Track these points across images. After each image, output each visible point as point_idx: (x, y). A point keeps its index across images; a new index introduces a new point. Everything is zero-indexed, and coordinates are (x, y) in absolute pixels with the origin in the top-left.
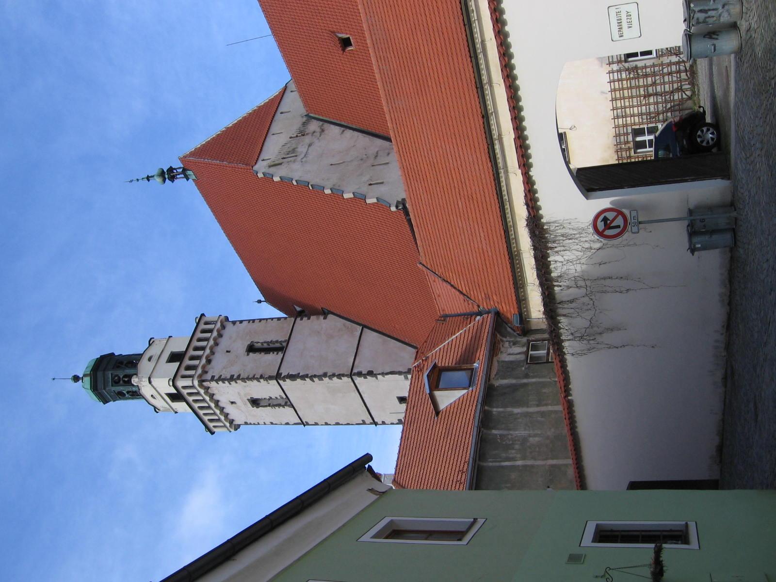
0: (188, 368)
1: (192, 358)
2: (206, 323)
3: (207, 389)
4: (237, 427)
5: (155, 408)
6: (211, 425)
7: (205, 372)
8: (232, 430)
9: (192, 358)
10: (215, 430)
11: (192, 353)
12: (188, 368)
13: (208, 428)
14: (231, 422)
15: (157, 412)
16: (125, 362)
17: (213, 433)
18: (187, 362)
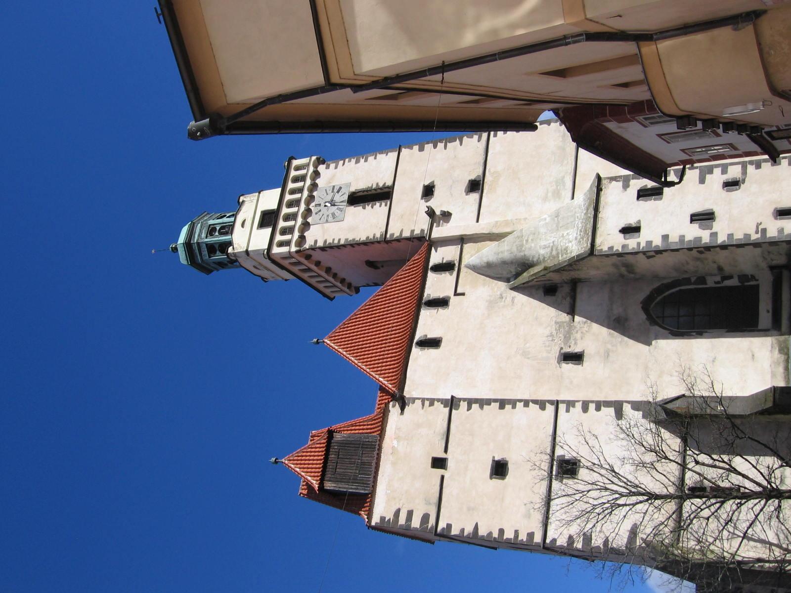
0: (284, 232)
1: (287, 218)
2: (298, 168)
3: (308, 257)
4: (357, 290)
5: (263, 278)
6: (328, 291)
7: (302, 238)
8: (355, 295)
9: (287, 218)
10: (332, 295)
11: (285, 210)
12: (284, 232)
13: (325, 295)
14: (349, 286)
15: (266, 282)
16: (218, 228)
17: (331, 299)
18: (282, 224)
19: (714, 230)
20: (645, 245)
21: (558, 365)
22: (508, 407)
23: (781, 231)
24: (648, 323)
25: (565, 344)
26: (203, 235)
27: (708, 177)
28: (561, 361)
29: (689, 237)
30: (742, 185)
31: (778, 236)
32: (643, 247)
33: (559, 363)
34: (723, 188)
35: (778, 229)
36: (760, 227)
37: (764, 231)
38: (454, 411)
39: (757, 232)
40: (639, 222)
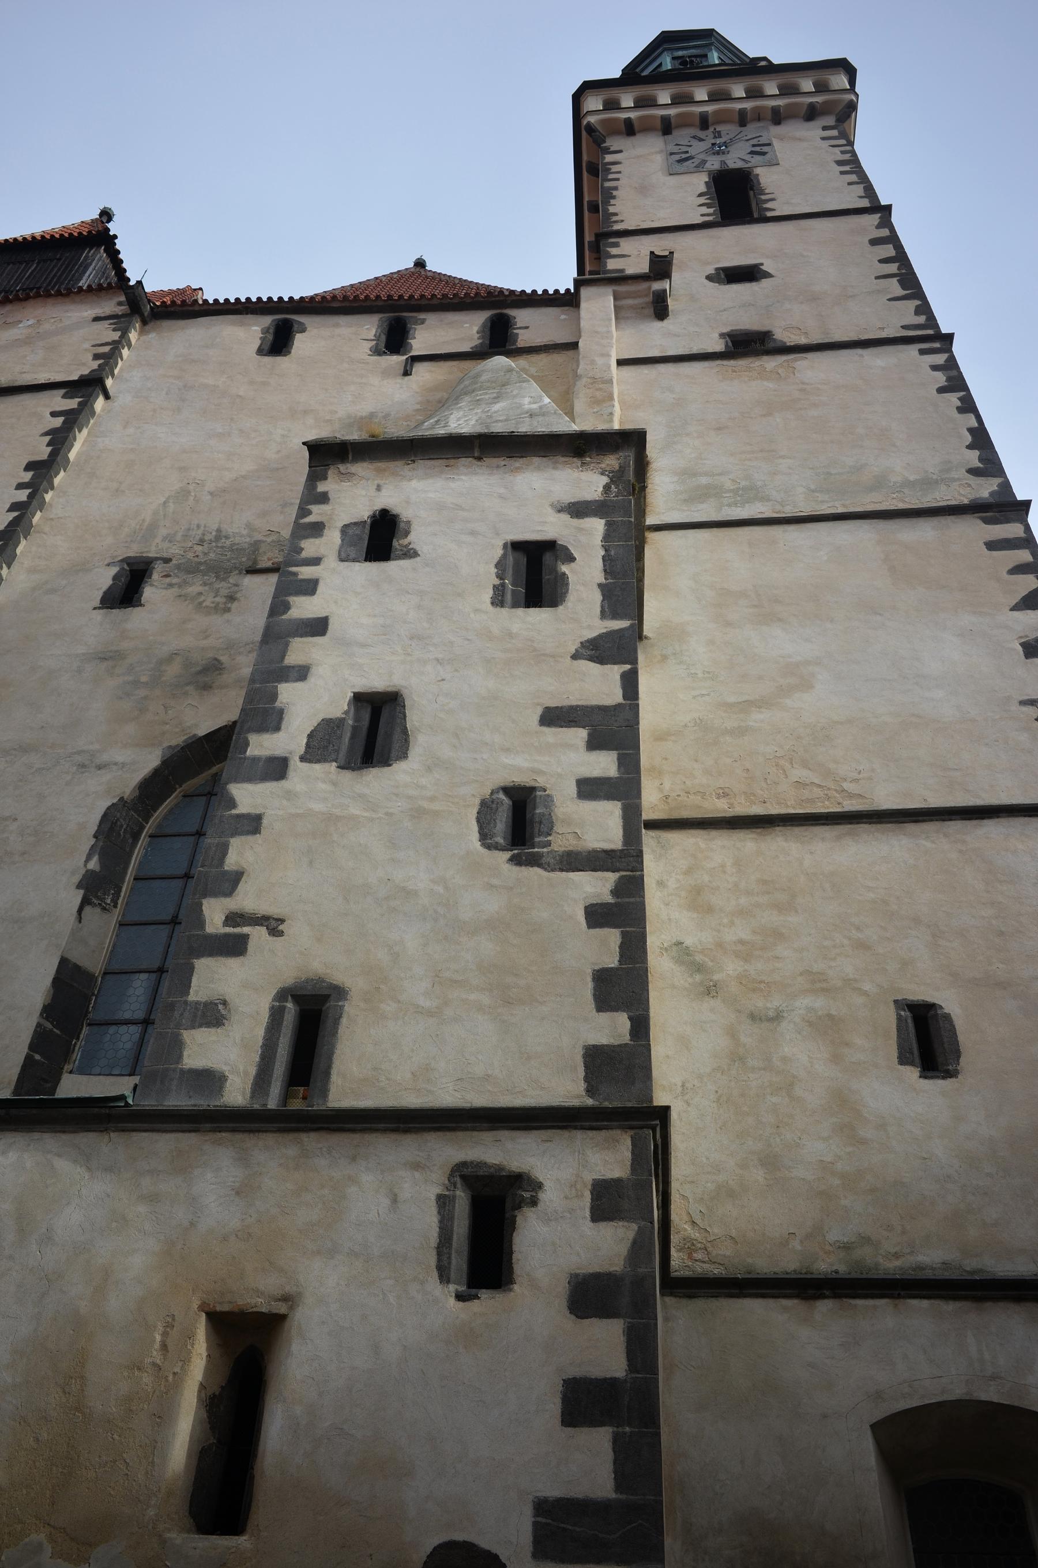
19: (295, 763)
20: (300, 577)
21: (120, 558)
22: (27, 477)
23: (213, 1015)
24: (179, 740)
25: (178, 567)
26: (680, 53)
27: (581, 735)
28: (128, 564)
29: (287, 693)
30: (508, 855)
31: (186, 1002)
32: (295, 574)
33: (122, 561)
34: (506, 790)
35: (225, 1003)
36: (257, 935)
37: (234, 946)
38: (62, 391)
39: (234, 918)
40: (410, 554)
